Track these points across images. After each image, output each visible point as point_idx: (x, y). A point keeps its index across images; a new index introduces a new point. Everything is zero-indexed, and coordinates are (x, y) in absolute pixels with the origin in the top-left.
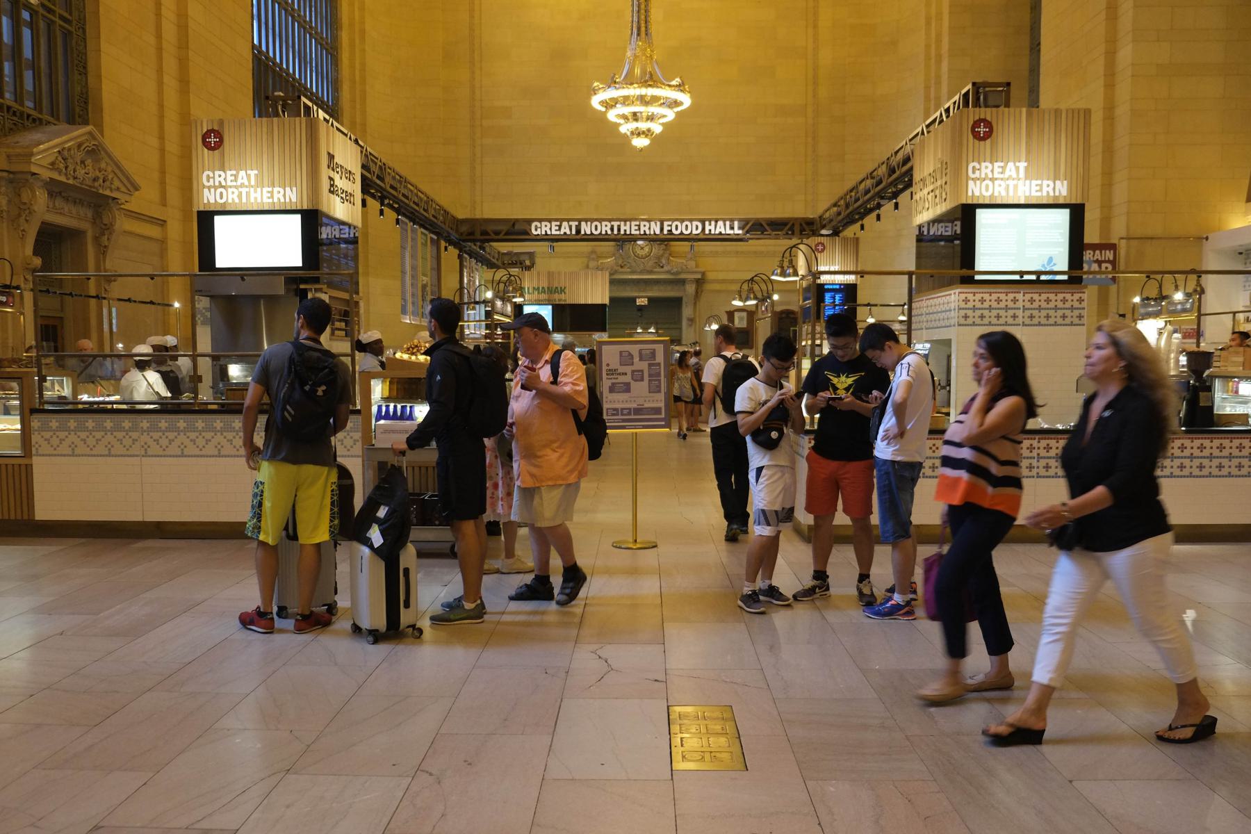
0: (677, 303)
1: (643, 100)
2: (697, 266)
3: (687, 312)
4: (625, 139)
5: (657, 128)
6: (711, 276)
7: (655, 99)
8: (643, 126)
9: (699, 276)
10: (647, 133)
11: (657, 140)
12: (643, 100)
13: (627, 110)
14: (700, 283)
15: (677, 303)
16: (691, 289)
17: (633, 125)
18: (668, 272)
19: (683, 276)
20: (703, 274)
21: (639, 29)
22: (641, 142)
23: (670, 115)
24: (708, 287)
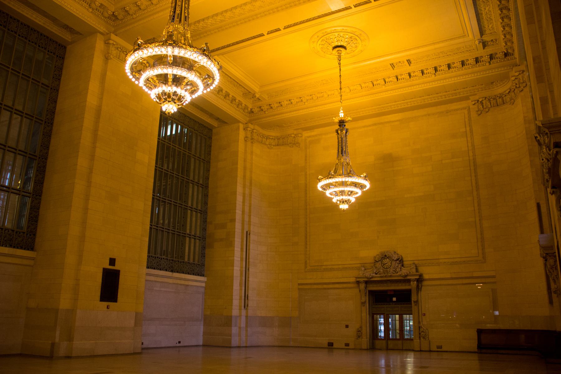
0: (409, 292)
1: (343, 184)
2: (417, 270)
3: (414, 298)
4: (336, 206)
5: (353, 199)
6: (426, 277)
9: (417, 277)
10: (347, 202)
11: (352, 206)
12: (343, 184)
13: (331, 190)
15: (409, 292)
16: (414, 284)
17: (340, 198)
18: (400, 276)
19: (408, 278)
20: (421, 275)
22: (344, 207)
23: (359, 192)
24: (425, 283)
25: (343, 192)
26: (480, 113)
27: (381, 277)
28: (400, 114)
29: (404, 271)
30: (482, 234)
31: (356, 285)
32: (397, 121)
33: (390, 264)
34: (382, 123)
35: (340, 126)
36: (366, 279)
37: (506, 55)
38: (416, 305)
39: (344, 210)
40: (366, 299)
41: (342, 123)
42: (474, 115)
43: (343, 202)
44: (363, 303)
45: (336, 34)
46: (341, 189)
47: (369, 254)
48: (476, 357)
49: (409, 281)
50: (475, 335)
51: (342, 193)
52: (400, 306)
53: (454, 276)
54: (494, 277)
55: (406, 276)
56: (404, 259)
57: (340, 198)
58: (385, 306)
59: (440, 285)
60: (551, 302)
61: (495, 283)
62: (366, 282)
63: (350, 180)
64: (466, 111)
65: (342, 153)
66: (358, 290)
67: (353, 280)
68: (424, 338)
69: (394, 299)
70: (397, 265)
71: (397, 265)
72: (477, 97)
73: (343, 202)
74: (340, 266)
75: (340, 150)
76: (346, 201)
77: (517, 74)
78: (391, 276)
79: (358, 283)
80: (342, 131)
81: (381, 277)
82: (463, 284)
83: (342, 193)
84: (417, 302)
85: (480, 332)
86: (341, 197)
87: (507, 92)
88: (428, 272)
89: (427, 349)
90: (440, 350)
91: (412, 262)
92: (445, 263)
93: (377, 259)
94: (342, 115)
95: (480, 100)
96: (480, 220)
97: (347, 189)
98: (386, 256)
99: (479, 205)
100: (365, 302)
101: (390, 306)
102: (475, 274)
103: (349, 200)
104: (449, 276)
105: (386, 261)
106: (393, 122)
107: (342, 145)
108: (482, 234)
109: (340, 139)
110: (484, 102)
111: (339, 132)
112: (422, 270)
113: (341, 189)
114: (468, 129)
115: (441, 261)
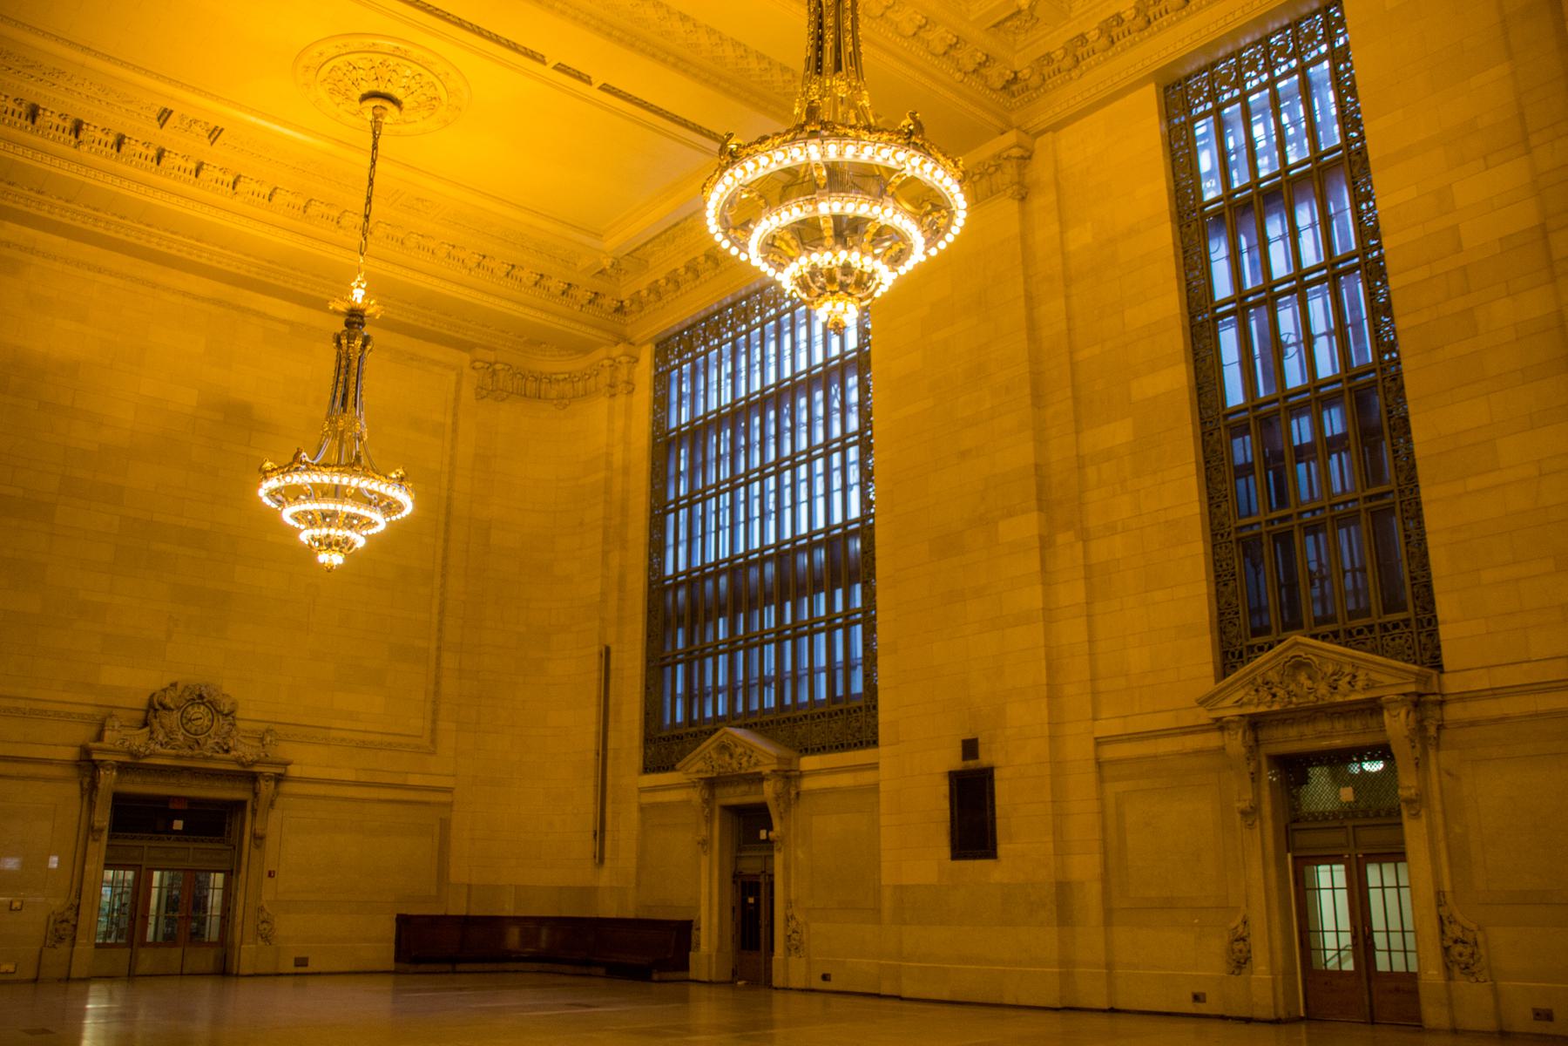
1: (337, 492)
6: (294, 771)
7: (359, 497)
8: (337, 533)
10: (330, 544)
12: (337, 492)
14: (279, 779)
17: (317, 532)
18: (237, 761)
19: (256, 769)
21: (345, 396)
24: (286, 787)
25: (337, 514)
26: (482, 393)
27: (178, 757)
28: (296, 307)
29: (246, 750)
30: (437, 683)
31: (72, 772)
32: (284, 322)
33: (207, 723)
34: (237, 308)
35: (348, 324)
36: (126, 759)
37: (620, 309)
38: (258, 847)
39: (330, 570)
40: (103, 818)
41: (355, 318)
42: (468, 392)
43: (330, 544)
44: (92, 830)
45: (378, 59)
46: (329, 506)
47: (133, 681)
48: (388, 983)
49: (253, 778)
50: (388, 928)
51: (328, 518)
52: (192, 845)
53: (363, 778)
54: (449, 790)
55: (254, 763)
56: (238, 714)
57: (317, 532)
58: (145, 843)
59: (325, 797)
60: (600, 859)
61: (451, 804)
62: (122, 768)
63: (296, 479)
64: (453, 376)
65: (344, 404)
66: (73, 790)
67: (71, 754)
68: (266, 938)
69: (178, 825)
70: (226, 728)
71: (226, 728)
72: (491, 356)
73: (329, 545)
74: (21, 704)
75: (339, 395)
76: (337, 544)
77: (624, 359)
78: (206, 758)
79: (87, 765)
80: (351, 339)
81: (178, 757)
82: (380, 801)
83: (328, 518)
84: (259, 839)
85: (403, 921)
86: (325, 531)
87: (561, 377)
88: (305, 761)
89: (270, 970)
90: (302, 970)
91: (263, 727)
92: (343, 740)
93: (167, 701)
94: (358, 295)
95: (498, 367)
96: (439, 648)
97: (348, 508)
98: (201, 697)
99: (442, 612)
100: (101, 830)
101: (162, 844)
102: (415, 780)
103: (346, 540)
104: (350, 776)
105: (199, 712)
106: (195, 297)
107: (346, 380)
108: (437, 683)
109: (344, 363)
110: (502, 374)
111: (344, 341)
112: (286, 751)
113: (329, 506)
114: (449, 421)
115: (333, 733)
